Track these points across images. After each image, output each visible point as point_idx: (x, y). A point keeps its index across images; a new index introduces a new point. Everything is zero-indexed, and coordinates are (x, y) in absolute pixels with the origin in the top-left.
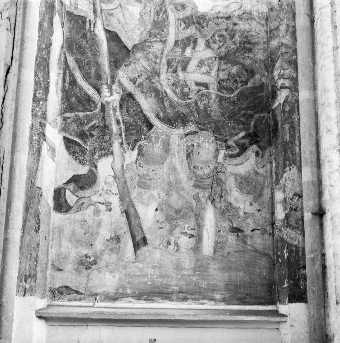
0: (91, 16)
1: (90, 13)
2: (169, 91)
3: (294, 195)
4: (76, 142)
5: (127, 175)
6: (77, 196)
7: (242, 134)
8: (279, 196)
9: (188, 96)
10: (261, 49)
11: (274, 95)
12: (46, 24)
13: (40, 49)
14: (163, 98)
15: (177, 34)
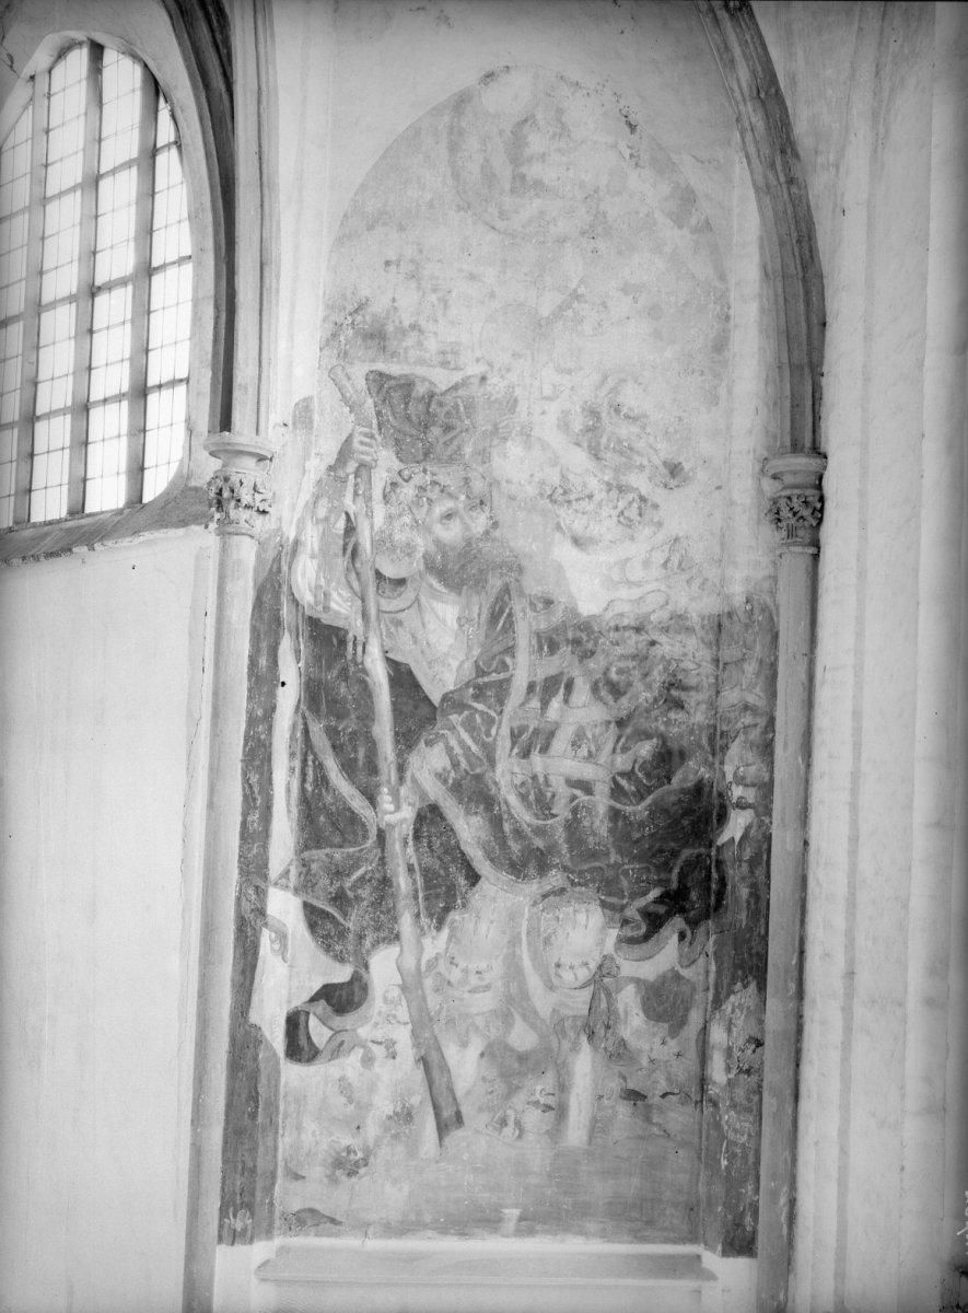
0: (356, 627)
1: (356, 620)
2: (513, 800)
3: (748, 1041)
4: (328, 914)
5: (428, 983)
6: (331, 1029)
7: (654, 893)
8: (717, 1035)
9: (550, 809)
10: (703, 701)
11: (722, 817)
12: (263, 661)
13: (252, 721)
14: (500, 815)
15: (532, 666)
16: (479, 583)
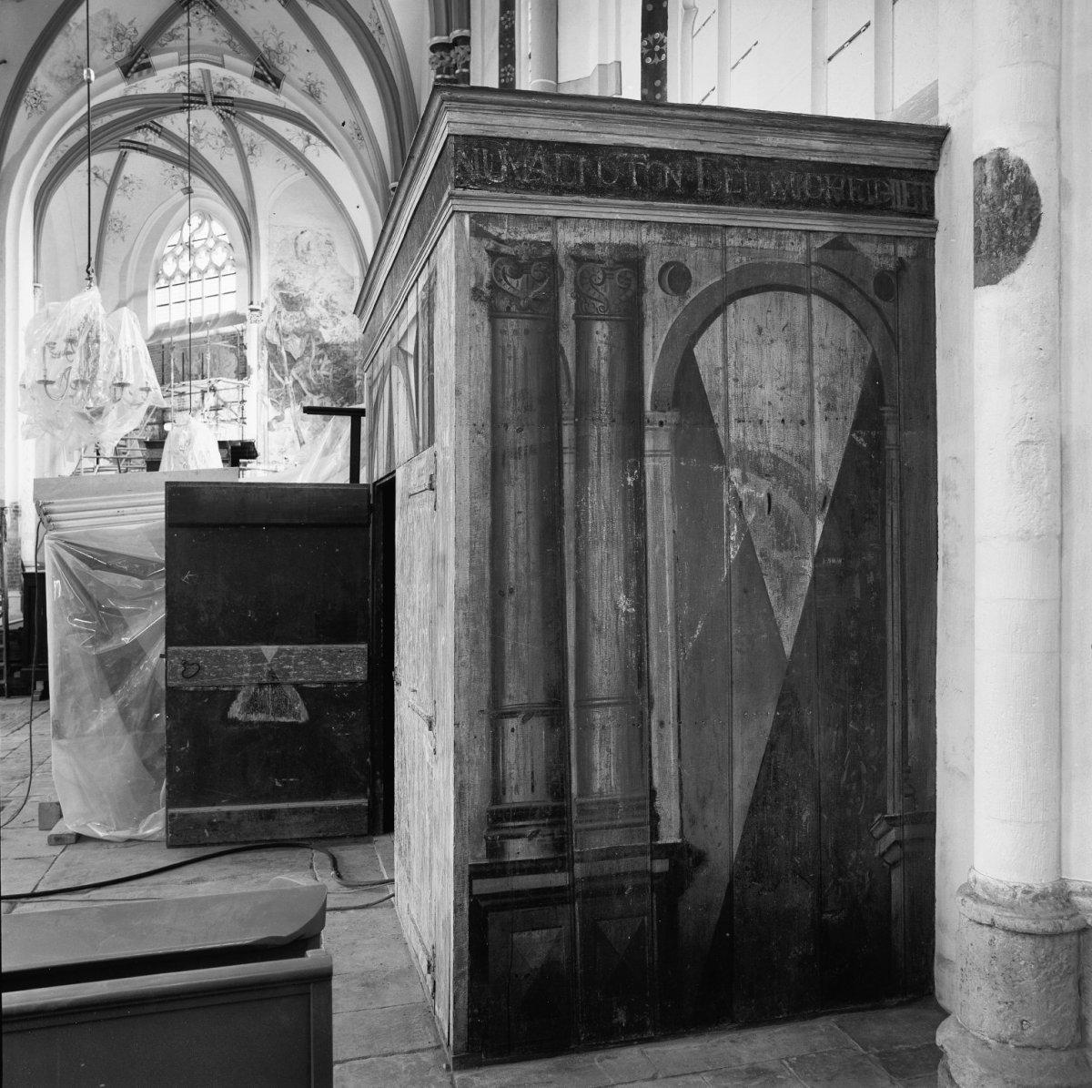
0: (279, 344)
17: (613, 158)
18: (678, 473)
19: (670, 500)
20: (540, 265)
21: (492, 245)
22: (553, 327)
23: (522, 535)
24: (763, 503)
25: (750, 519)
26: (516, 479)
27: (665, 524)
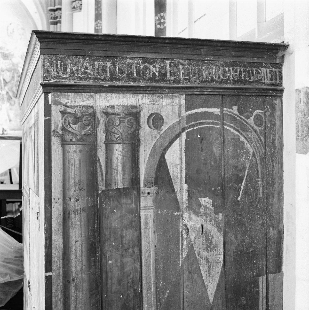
16: (11, 71)
17: (124, 63)
18: (157, 218)
19: (153, 231)
20: (87, 118)
21: (63, 108)
22: (94, 147)
23: (79, 252)
24: (199, 229)
25: (192, 237)
26: (75, 225)
27: (151, 243)
